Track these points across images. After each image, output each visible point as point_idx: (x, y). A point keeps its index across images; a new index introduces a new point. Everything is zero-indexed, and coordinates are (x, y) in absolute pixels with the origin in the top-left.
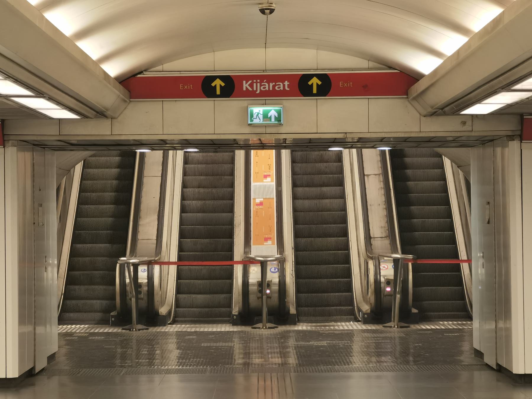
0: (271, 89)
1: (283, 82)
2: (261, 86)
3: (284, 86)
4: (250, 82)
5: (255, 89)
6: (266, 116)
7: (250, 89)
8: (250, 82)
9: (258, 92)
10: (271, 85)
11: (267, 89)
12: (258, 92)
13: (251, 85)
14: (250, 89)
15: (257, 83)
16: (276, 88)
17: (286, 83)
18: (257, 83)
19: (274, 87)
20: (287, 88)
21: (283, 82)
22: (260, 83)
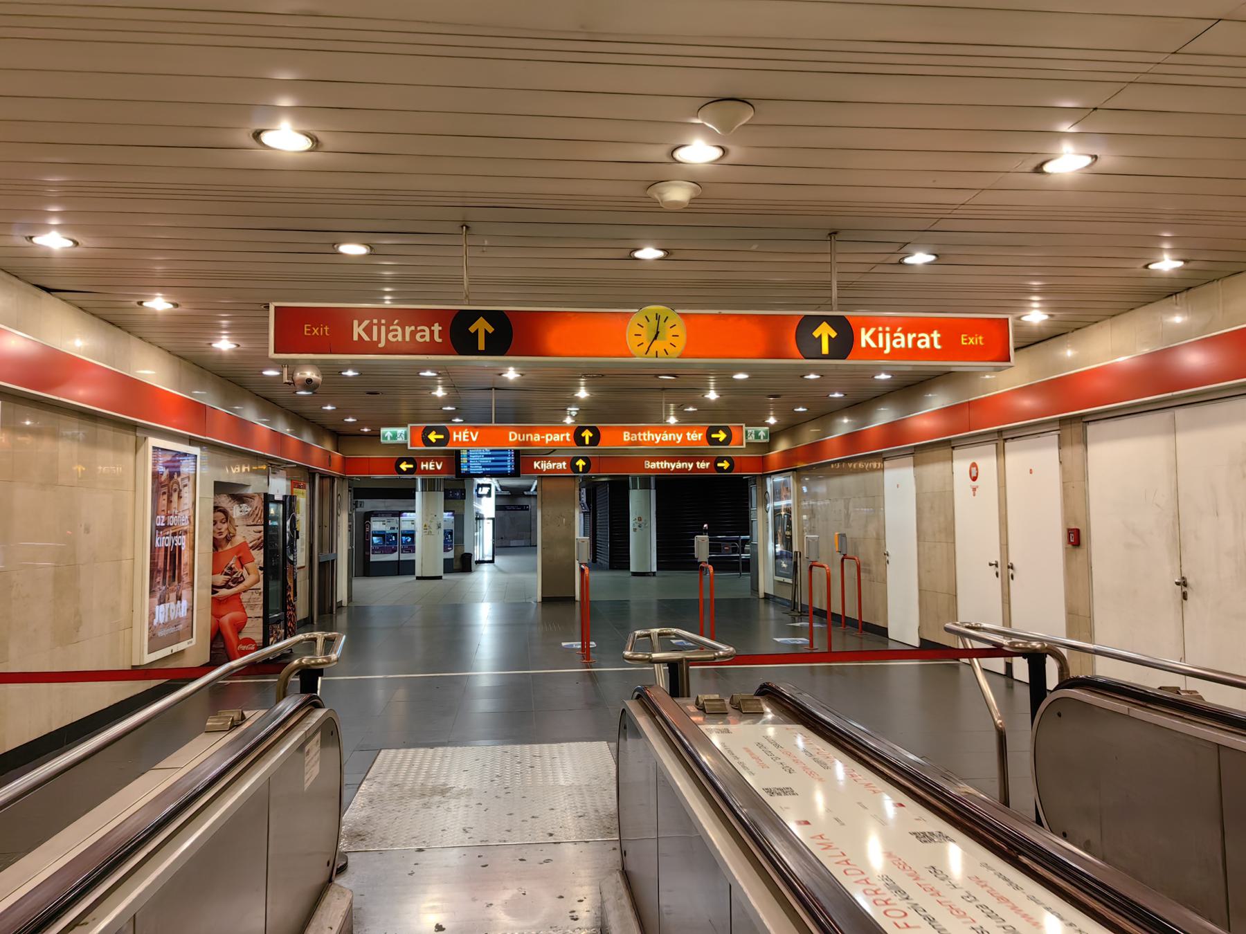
0: (910, 345)
1: (930, 332)
2: (892, 338)
3: (932, 340)
4: (872, 331)
5: (881, 345)
6: (394, 436)
7: (873, 345)
8: (872, 331)
9: (887, 351)
10: (911, 337)
11: (903, 345)
12: (887, 351)
13: (874, 337)
14: (873, 345)
15: (884, 332)
16: (919, 344)
17: (936, 335)
18: (884, 332)
19: (915, 340)
20: (937, 346)
21: (930, 332)
22: (892, 332)
